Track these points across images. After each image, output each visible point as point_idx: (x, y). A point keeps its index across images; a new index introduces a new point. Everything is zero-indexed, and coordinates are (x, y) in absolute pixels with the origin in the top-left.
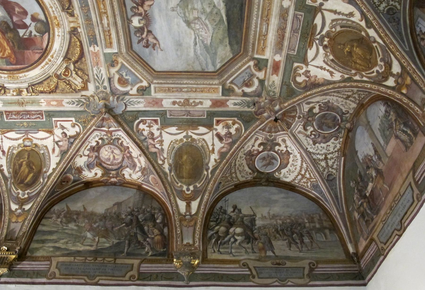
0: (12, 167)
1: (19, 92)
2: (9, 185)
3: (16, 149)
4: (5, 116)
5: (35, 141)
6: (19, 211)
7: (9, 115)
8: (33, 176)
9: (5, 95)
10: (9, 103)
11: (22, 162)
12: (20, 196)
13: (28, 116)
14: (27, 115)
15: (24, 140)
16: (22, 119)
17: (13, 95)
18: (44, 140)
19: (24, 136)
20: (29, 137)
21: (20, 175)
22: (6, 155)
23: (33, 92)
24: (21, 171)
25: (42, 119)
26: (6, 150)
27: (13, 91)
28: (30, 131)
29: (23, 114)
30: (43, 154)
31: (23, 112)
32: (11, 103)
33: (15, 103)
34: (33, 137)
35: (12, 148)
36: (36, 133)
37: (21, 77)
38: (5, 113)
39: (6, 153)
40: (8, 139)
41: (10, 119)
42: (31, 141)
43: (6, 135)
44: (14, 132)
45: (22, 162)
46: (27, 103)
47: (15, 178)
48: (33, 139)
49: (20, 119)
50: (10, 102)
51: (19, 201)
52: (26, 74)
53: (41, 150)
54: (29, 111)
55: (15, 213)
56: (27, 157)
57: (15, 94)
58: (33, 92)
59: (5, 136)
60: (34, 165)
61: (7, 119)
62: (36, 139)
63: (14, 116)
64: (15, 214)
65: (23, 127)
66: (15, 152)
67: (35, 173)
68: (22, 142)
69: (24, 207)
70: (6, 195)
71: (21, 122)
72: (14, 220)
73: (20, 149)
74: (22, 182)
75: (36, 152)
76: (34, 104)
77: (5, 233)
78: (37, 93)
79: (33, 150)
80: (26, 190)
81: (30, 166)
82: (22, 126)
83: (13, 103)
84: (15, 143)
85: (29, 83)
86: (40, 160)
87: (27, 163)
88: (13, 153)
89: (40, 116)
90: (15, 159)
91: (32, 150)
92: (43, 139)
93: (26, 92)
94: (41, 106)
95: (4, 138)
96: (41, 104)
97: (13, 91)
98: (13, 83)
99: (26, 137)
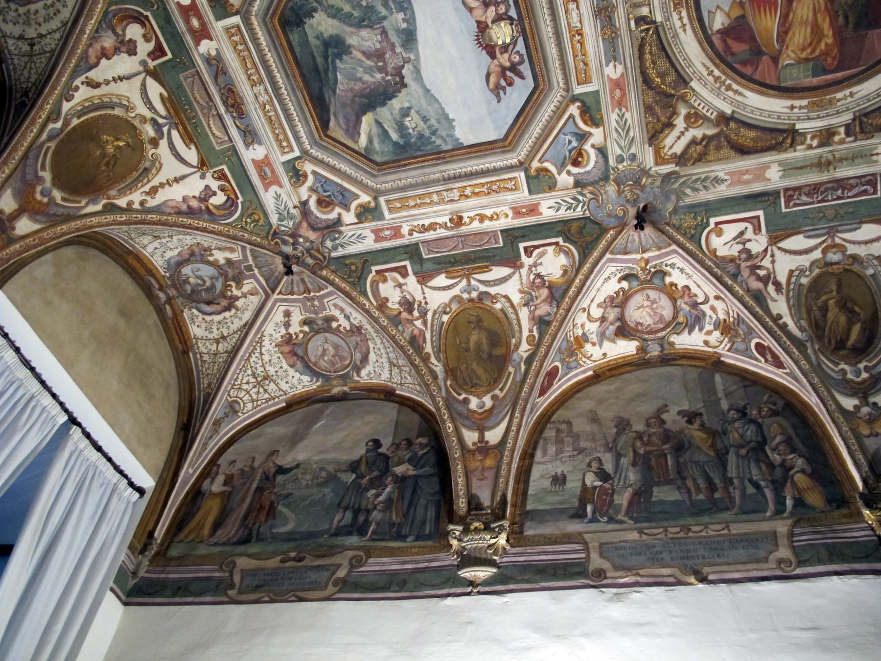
0: (805, 316)
1: (826, 136)
2: (813, 358)
3: (808, 273)
4: (782, 200)
5: (852, 250)
6: (865, 410)
7: (792, 196)
8: (863, 330)
9: (792, 149)
10: (798, 168)
11: (826, 303)
12: (850, 376)
13: (840, 192)
14: (836, 190)
15: (824, 252)
16: (823, 201)
17: (810, 147)
18: (875, 244)
19: (823, 242)
20: (838, 240)
21: (830, 329)
22: (784, 291)
23: (862, 131)
24: (829, 324)
25: (874, 193)
26: (782, 278)
27: (812, 138)
28: (840, 228)
29: (827, 189)
30: (872, 276)
31: (829, 185)
32: (801, 168)
33: (812, 166)
34: (845, 240)
35: (796, 273)
36: (855, 229)
37: (839, 100)
38: (785, 194)
39: (784, 287)
40: (787, 254)
41: (796, 205)
42: (842, 249)
43: (781, 245)
44: (801, 236)
45: (826, 303)
46: (841, 160)
47: (820, 338)
48: (847, 245)
49: (819, 202)
50: (799, 165)
51: (853, 388)
52: (854, 89)
53: (866, 268)
54: (843, 180)
55: (859, 415)
56: (834, 288)
57: (815, 143)
58: (862, 131)
59: (779, 248)
60: (856, 304)
61: (787, 207)
62: (854, 243)
63: (805, 199)
64: (860, 418)
65: (824, 220)
66: (804, 281)
67: (865, 322)
68: (820, 256)
69: (872, 400)
70: (816, 380)
71: (819, 210)
72: (865, 430)
73: (817, 271)
74: (840, 345)
75: (855, 273)
76: (857, 161)
77: (863, 460)
78: (870, 132)
79: (850, 271)
80: (860, 362)
81: (848, 309)
82: (821, 218)
83: (806, 167)
84: (805, 261)
85: (854, 113)
86: (867, 291)
87: (837, 302)
88: (801, 285)
89: (868, 187)
90: (806, 297)
91: (846, 270)
92: (872, 241)
93: (843, 135)
94: (876, 161)
95: (777, 253)
96: (875, 158)
97: (812, 138)
98: (818, 117)
99: (829, 241)
